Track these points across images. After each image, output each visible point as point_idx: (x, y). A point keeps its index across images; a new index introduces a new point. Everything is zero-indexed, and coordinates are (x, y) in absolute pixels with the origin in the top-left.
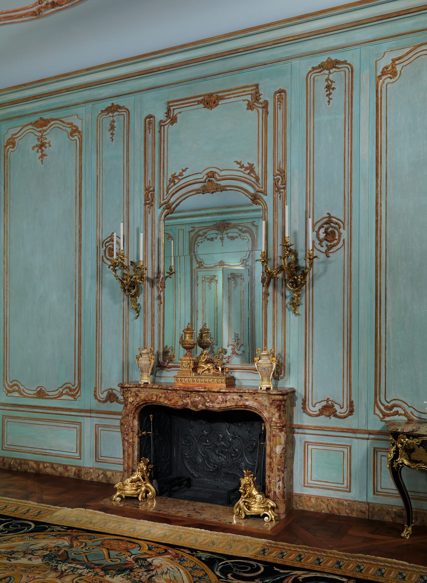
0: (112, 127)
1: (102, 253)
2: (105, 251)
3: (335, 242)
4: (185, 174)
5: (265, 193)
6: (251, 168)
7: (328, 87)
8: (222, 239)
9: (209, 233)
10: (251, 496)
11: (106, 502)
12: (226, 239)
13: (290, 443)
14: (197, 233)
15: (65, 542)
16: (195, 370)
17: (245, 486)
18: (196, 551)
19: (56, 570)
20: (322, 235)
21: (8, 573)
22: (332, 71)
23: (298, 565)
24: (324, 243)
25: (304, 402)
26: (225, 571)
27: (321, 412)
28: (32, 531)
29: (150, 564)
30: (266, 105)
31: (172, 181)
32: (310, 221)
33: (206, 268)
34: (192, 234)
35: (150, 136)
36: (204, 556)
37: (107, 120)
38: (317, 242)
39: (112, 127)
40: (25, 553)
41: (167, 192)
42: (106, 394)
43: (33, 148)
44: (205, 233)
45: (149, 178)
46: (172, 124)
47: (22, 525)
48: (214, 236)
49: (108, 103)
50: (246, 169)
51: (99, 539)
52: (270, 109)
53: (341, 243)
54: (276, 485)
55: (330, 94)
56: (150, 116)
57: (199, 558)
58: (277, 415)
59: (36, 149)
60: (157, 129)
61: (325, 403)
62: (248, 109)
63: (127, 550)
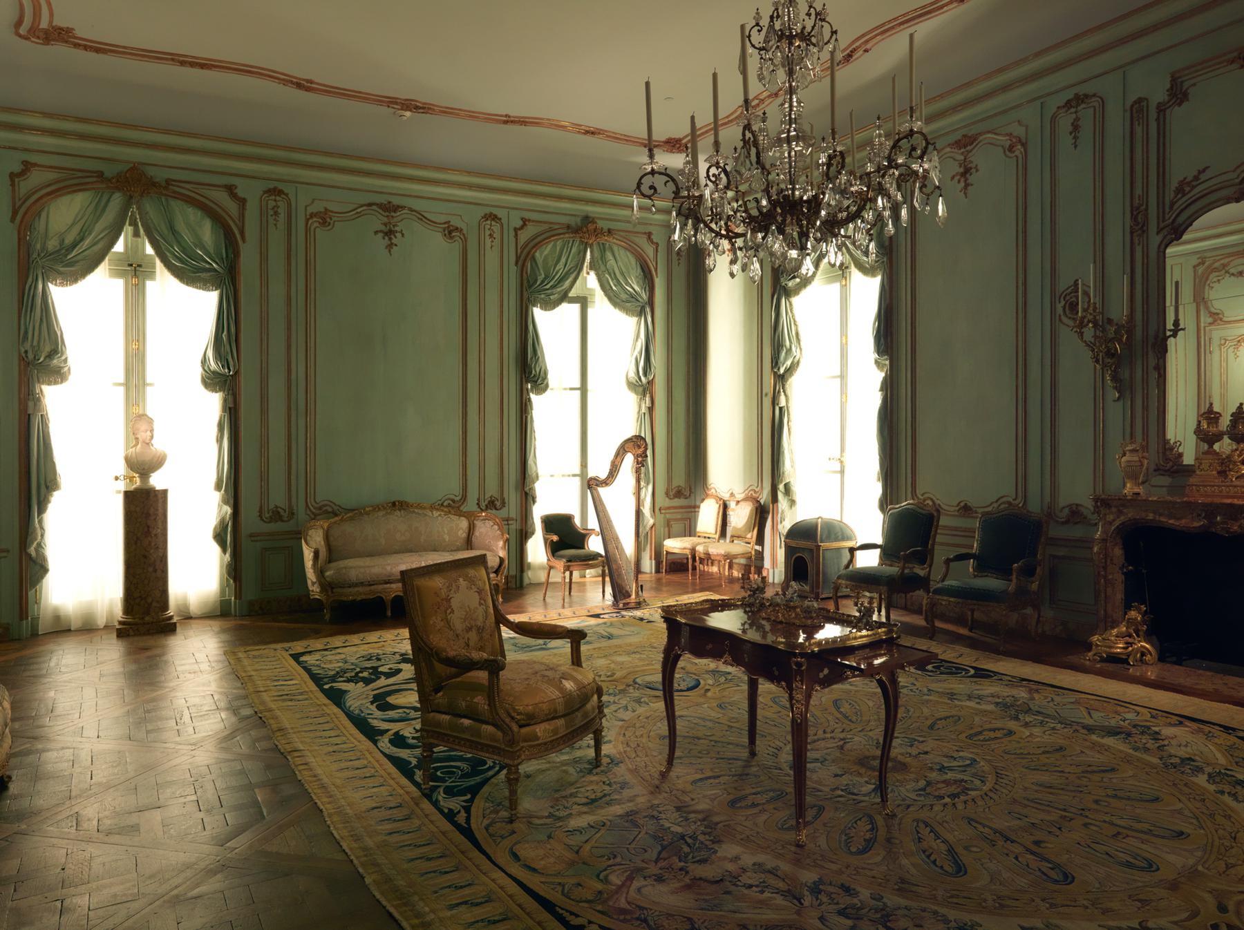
0: (1076, 127)
2: (1064, 308)
9: (1232, 264)
11: (1073, 659)
14: (1209, 267)
15: (1022, 694)
16: (1223, 473)
18: (1234, 729)
19: (1017, 718)
21: (954, 713)
28: (972, 676)
29: (1157, 733)
33: (1229, 322)
34: (1201, 270)
40: (970, 697)
42: (1066, 511)
44: (1224, 266)
47: (957, 668)
51: (1072, 697)
59: (957, 178)
63: (1116, 712)
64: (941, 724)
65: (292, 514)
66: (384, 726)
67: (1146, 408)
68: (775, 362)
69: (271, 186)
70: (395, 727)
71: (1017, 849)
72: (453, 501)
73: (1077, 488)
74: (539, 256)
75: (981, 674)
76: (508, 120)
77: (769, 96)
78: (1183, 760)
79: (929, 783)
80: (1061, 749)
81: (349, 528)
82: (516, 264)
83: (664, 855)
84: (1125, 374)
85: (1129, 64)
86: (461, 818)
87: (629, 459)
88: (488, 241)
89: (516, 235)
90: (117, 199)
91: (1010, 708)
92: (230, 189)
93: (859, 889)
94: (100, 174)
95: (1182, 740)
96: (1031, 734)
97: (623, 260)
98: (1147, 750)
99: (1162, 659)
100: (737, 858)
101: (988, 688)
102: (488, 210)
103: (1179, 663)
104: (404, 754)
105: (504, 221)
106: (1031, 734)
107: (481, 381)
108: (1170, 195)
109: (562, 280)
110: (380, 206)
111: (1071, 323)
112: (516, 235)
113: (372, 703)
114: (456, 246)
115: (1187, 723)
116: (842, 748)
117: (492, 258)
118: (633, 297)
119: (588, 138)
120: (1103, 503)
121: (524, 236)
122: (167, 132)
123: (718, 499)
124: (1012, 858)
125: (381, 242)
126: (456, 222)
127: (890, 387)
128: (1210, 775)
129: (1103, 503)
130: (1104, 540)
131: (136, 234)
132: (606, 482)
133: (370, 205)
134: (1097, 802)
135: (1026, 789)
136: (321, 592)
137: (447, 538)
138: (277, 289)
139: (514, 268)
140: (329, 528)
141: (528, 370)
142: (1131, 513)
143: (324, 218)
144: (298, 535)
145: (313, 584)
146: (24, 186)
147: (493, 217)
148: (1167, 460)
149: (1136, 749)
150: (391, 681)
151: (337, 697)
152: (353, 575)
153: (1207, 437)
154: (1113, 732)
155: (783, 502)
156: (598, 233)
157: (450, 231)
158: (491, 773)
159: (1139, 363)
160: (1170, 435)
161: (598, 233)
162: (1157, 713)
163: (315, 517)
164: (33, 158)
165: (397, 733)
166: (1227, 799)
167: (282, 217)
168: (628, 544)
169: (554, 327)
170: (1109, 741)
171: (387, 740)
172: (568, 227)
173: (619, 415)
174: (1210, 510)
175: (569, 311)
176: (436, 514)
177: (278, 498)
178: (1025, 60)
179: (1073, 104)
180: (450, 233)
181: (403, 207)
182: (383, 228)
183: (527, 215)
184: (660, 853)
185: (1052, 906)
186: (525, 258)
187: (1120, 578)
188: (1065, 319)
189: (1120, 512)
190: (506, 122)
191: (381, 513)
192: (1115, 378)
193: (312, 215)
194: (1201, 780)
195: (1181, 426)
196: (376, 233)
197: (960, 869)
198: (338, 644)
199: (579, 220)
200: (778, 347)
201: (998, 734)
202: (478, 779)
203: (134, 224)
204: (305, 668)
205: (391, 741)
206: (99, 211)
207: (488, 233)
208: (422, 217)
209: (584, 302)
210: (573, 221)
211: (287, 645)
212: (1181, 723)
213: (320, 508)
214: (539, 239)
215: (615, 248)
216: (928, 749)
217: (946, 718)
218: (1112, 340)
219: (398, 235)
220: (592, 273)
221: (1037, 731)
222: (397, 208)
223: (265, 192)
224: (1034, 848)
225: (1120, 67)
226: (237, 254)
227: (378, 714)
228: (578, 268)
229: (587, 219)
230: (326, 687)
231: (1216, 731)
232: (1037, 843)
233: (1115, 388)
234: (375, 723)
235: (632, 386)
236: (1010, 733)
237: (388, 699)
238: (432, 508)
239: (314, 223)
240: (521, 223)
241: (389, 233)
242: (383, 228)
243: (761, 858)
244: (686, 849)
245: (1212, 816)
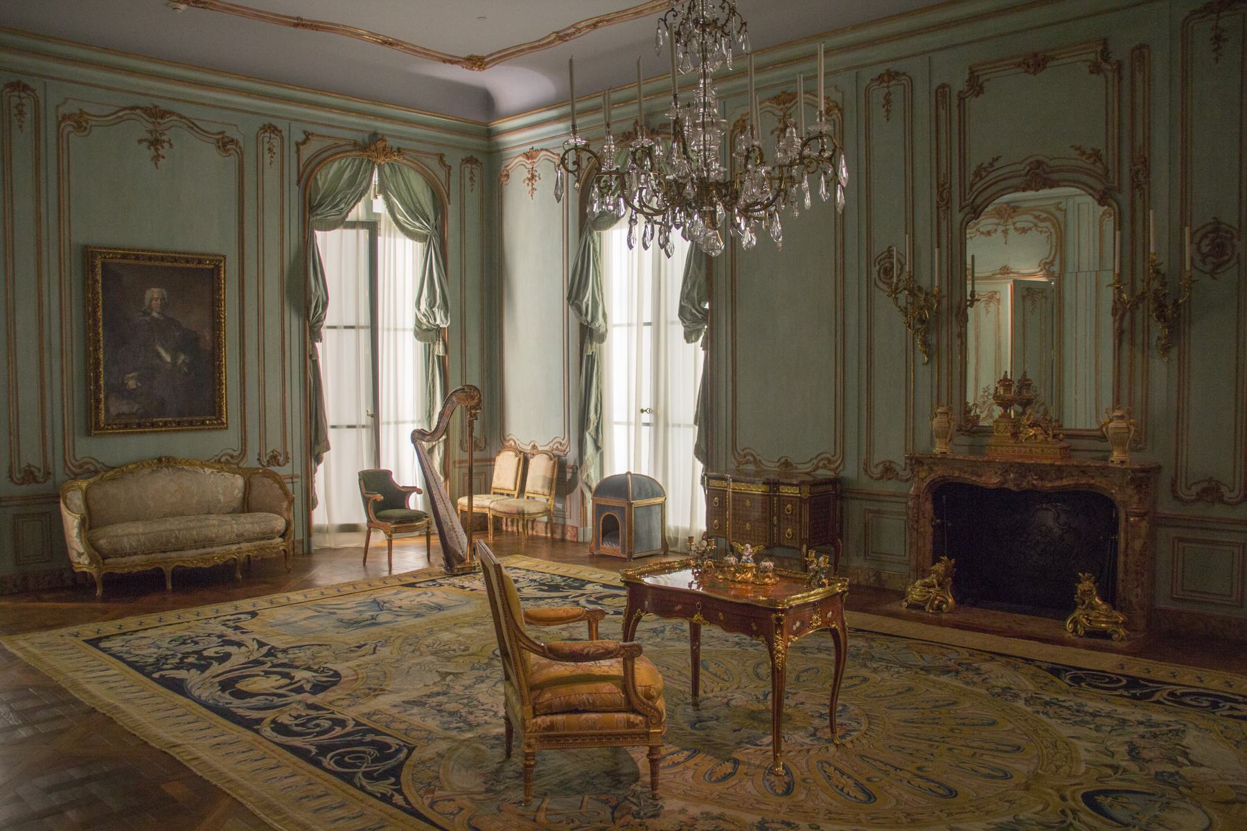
1: (875, 275)
3: (1226, 258)
4: (997, 165)
5: (1120, 191)
6: (1096, 156)
8: (1005, 232)
10: (1092, 607)
12: (1011, 231)
16: (1015, 435)
17: (1084, 593)
19: (865, 666)
20: (1205, 249)
22: (1221, 14)
23: (1172, 681)
24: (1210, 259)
25: (1174, 484)
26: (1077, 680)
27: (1200, 497)
30: (1120, 66)
31: (977, 174)
32: (1187, 229)
35: (942, 113)
36: (1044, 666)
38: (1197, 258)
39: (888, 101)
41: (971, 189)
43: (772, 133)
45: (943, 171)
46: (977, 96)
48: (989, 228)
49: (881, 69)
50: (1090, 156)
52: (1126, 73)
53: (1234, 260)
55: (1219, 48)
56: (943, 86)
57: (1040, 667)
58: (1136, 498)
60: (955, 102)
61: (1205, 485)
62: (1092, 72)
64: (804, 676)
65: (48, 474)
66: (255, 715)
67: (950, 373)
69: (13, 80)
70: (270, 715)
71: (909, 776)
72: (232, 457)
76: (299, 23)
77: (587, 27)
78: (1004, 689)
79: (816, 729)
80: (910, 689)
81: (111, 489)
82: (299, 182)
83: (617, 814)
84: (933, 339)
85: (934, 50)
86: (398, 799)
88: (267, 156)
89: (298, 150)
93: (797, 823)
96: (882, 679)
98: (975, 684)
99: (960, 601)
100: (683, 811)
102: (266, 121)
103: (974, 605)
104: (297, 742)
105: (285, 134)
106: (882, 679)
108: (970, 177)
110: (145, 110)
111: (885, 287)
112: (298, 150)
113: (223, 690)
114: (233, 160)
115: (997, 658)
116: (727, 704)
117: (271, 175)
119: (386, 48)
121: (307, 152)
123: (518, 452)
124: (905, 782)
126: (231, 133)
128: (1026, 700)
129: (916, 461)
130: (918, 496)
133: (133, 108)
134: (952, 730)
135: (895, 725)
136: (90, 564)
137: (221, 498)
139: (295, 188)
140: (88, 488)
142: (939, 471)
143: (80, 122)
144: (54, 498)
145: (80, 555)
147: (273, 129)
148: (968, 421)
149: (967, 683)
150: (227, 666)
151: (178, 687)
152: (126, 543)
154: (946, 671)
157: (225, 144)
158: (402, 756)
159: (944, 329)
160: (970, 399)
161: (387, 152)
162: (973, 651)
163: (76, 477)
165: (274, 721)
166: (1041, 716)
167: (29, 116)
170: (944, 679)
171: (268, 729)
172: (355, 144)
174: (1007, 467)
176: (208, 471)
177: (30, 455)
178: (843, 30)
179: (886, 78)
180: (224, 145)
181: (171, 113)
182: (148, 136)
183: (310, 128)
184: (613, 813)
185: (949, 815)
186: (306, 178)
187: (930, 530)
188: (881, 285)
189: (931, 470)
190: (296, 25)
191: (147, 471)
192: (925, 343)
193: (65, 118)
194: (1021, 704)
196: (140, 141)
197: (871, 797)
198: (134, 627)
199: (366, 136)
201: (856, 681)
202: (392, 762)
204: (113, 655)
205: (273, 729)
207: (267, 146)
208: (192, 126)
210: (362, 138)
211: (74, 629)
212: (993, 659)
213: (81, 467)
214: (324, 156)
215: (406, 170)
216: (802, 700)
217: (806, 671)
218: (922, 308)
219: (166, 145)
220: (380, 197)
221: (886, 675)
222: (164, 114)
223: (7, 86)
224: (920, 773)
225: (924, 53)
227: (236, 702)
229: (375, 137)
230: (156, 675)
231: (1020, 663)
232: (919, 769)
233: (925, 352)
234: (240, 712)
236: (865, 680)
237: (238, 686)
238: (203, 465)
239: (68, 127)
240: (303, 137)
241: (155, 143)
242: (148, 136)
243: (707, 808)
244: (635, 808)
245: (1035, 731)
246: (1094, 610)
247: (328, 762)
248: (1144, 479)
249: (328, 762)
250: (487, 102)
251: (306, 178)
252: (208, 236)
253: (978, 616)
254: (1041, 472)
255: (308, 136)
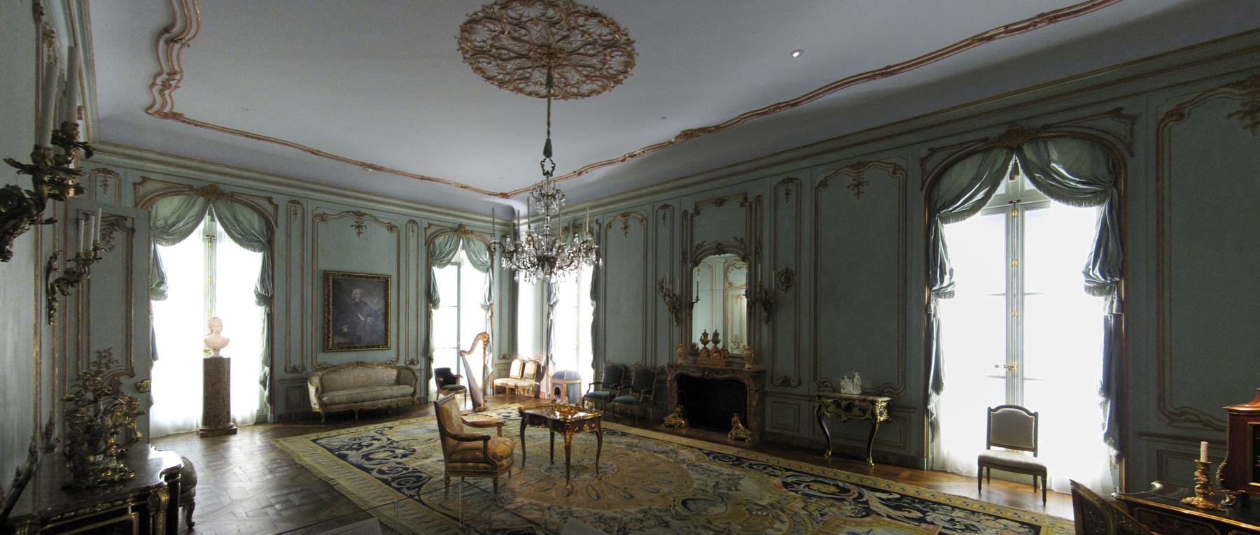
7: (787, 194)
13: (762, 401)
15: (636, 441)
37: (661, 213)
54: (753, 424)
68: (549, 299)
73: (663, 361)
74: (437, 241)
75: (624, 434)
87: (480, 343)
90: (201, 200)
91: (629, 446)
92: (270, 200)
94: (191, 187)
95: (685, 454)
97: (479, 246)
101: (624, 440)
104: (385, 477)
107: (407, 302)
109: (448, 254)
114: (394, 236)
117: (413, 241)
118: (483, 264)
120: (671, 366)
121: (429, 232)
122: (233, 168)
125: (354, 231)
126: (394, 223)
127: (596, 313)
131: (213, 220)
132: (469, 353)
138: (296, 252)
141: (431, 299)
142: (679, 371)
143: (323, 218)
146: (142, 190)
147: (414, 222)
153: (705, 342)
154: (663, 452)
155: (550, 364)
156: (466, 232)
157: (391, 228)
161: (466, 232)
164: (148, 175)
167: (299, 215)
168: (479, 382)
169: (443, 277)
173: (477, 320)
174: (704, 370)
175: (451, 269)
186: (429, 242)
194: (684, 466)
195: (696, 338)
200: (550, 293)
203: (211, 214)
206: (190, 207)
208: (376, 220)
209: (459, 265)
222: (363, 214)
226: (273, 233)
228: (456, 248)
229: (461, 226)
235: (483, 306)
239: (318, 220)
241: (359, 227)
246: (739, 429)
247: (394, 484)
248: (758, 375)
249: (394, 484)
250: (512, 212)
251: (429, 242)
252: (383, 266)
253: (694, 432)
254: (717, 372)
255: (430, 225)
